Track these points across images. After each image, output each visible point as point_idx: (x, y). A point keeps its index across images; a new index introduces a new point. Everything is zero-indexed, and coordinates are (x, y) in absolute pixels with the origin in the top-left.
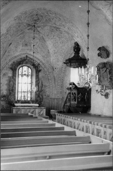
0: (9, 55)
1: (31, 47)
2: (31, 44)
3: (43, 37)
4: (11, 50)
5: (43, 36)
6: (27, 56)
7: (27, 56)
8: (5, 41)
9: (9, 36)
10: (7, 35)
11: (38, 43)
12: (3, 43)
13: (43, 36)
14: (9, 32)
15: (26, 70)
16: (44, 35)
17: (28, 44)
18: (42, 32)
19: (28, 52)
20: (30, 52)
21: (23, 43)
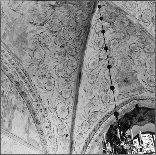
0: (95, 112)
1: (139, 83)
2: (135, 74)
3: (140, 25)
4: (96, 98)
5: (142, 23)
6: (137, 105)
7: (137, 105)
8: (69, 73)
9: (72, 58)
10: (67, 59)
11: (147, 64)
12: (66, 80)
13: (142, 23)
14: (66, 48)
15: (148, 141)
16: (143, 21)
17: (130, 78)
18: (132, 13)
19: (137, 95)
20: (142, 95)
21: (118, 78)
